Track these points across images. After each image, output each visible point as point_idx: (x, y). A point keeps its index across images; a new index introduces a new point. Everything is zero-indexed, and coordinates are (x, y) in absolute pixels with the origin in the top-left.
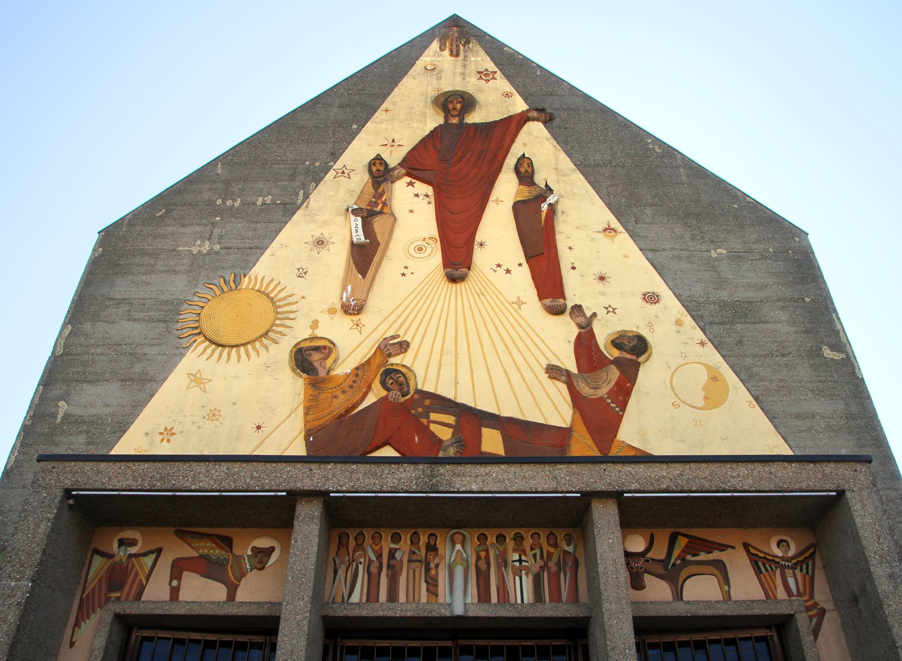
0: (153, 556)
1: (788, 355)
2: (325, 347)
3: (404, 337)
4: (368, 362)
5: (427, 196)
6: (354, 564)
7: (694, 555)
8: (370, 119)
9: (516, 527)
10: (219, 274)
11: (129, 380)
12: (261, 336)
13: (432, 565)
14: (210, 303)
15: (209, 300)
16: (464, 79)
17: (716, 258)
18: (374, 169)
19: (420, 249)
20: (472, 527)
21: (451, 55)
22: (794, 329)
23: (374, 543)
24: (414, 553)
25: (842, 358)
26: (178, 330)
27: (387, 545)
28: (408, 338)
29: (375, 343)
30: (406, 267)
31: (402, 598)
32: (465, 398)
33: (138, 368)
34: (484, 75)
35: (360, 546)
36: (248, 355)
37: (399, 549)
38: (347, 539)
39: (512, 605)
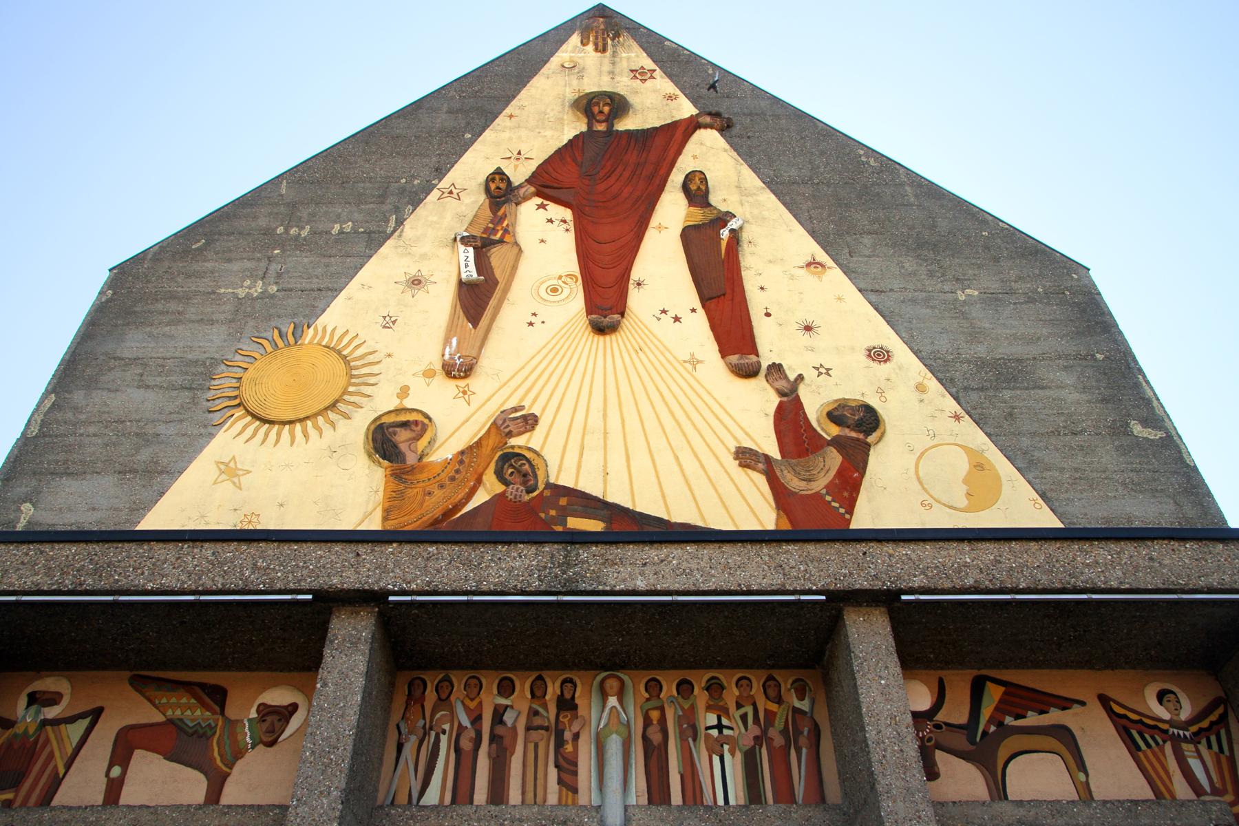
0: (83, 724)
1: (1081, 432)
2: (416, 423)
3: (530, 407)
4: (479, 444)
5: (564, 221)
6: (433, 734)
7: (1018, 717)
8: (488, 126)
9: (710, 667)
10: (273, 324)
11: (130, 472)
12: (326, 409)
13: (568, 735)
14: (257, 363)
15: (256, 359)
16: (613, 78)
17: (964, 301)
18: (493, 186)
19: (555, 290)
20: (636, 667)
21: (596, 50)
22: (1084, 397)
23: (467, 696)
24: (536, 713)
25: (1161, 438)
26: (208, 400)
27: (490, 699)
28: (536, 410)
29: (489, 418)
30: (534, 314)
31: (514, 796)
32: (617, 496)
34: (639, 74)
35: (444, 701)
36: (306, 435)
37: (512, 707)
38: (422, 687)
39: (708, 808)
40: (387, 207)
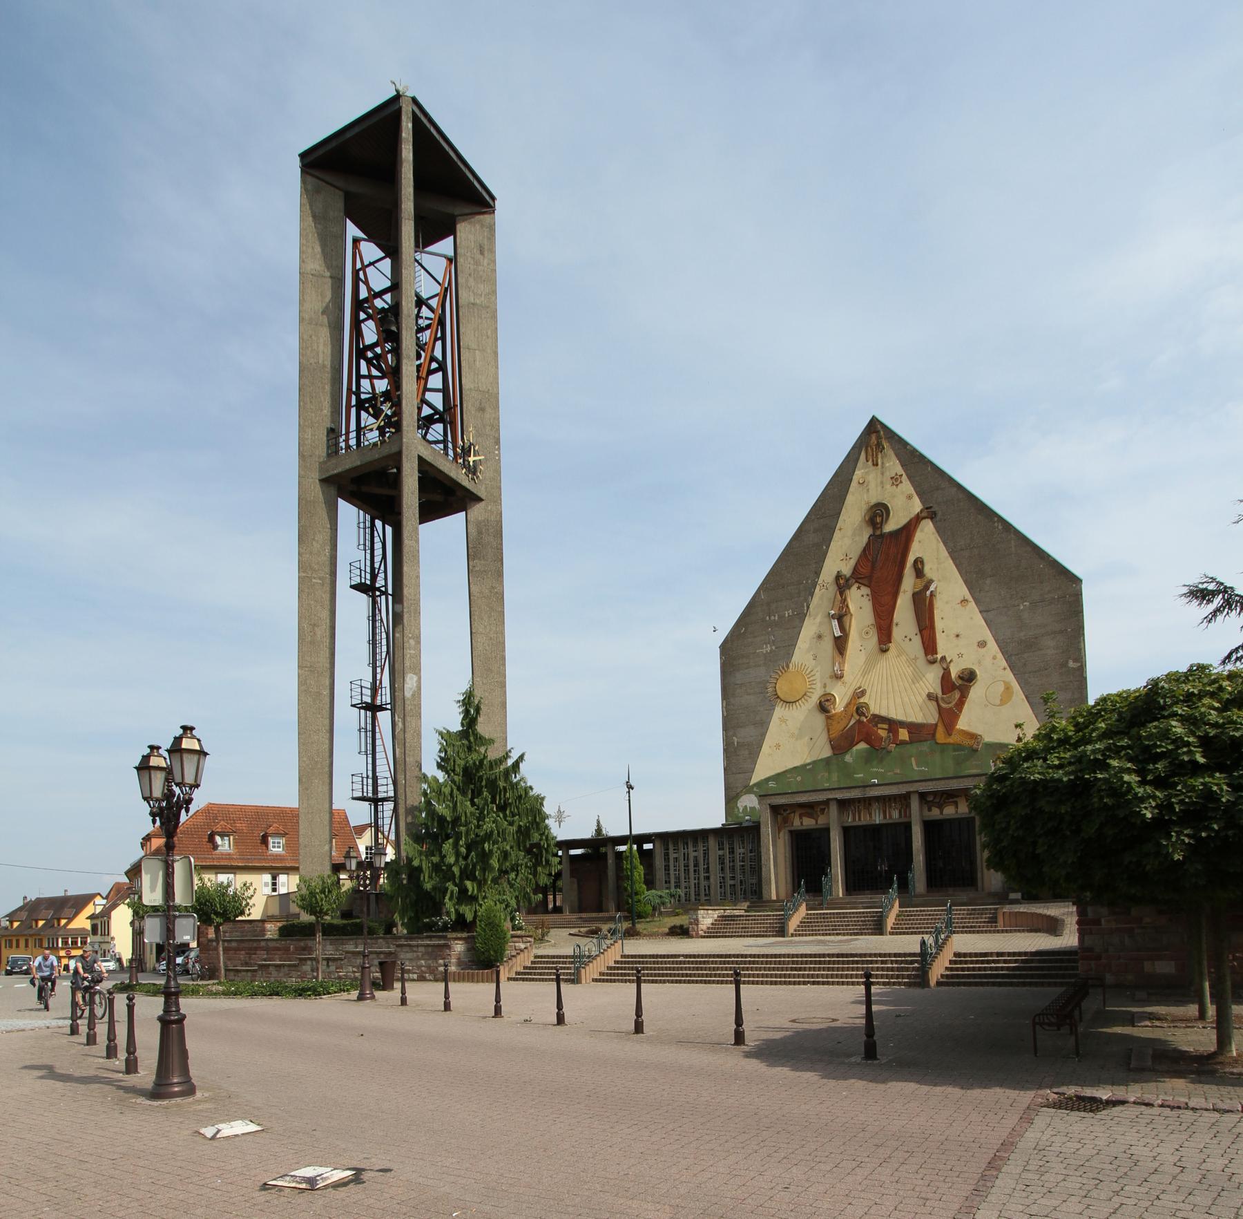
19: (867, 633)
40: (802, 598)
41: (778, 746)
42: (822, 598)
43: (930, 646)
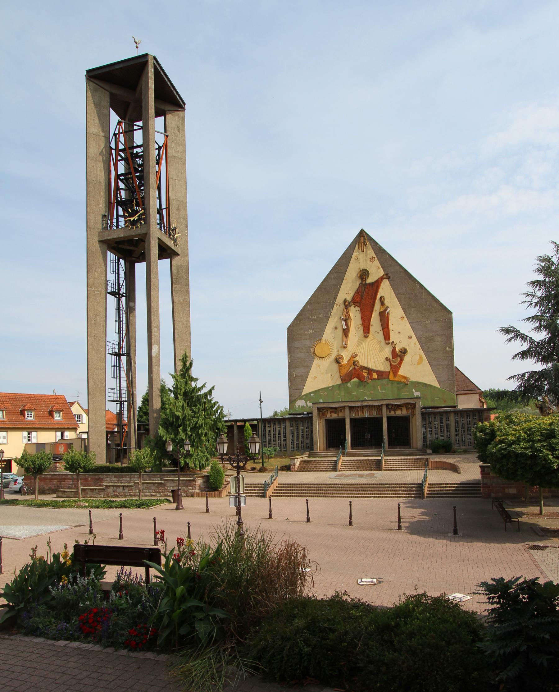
33: (306, 364)
40: (328, 310)
41: (315, 378)
42: (337, 310)
43: (387, 336)
